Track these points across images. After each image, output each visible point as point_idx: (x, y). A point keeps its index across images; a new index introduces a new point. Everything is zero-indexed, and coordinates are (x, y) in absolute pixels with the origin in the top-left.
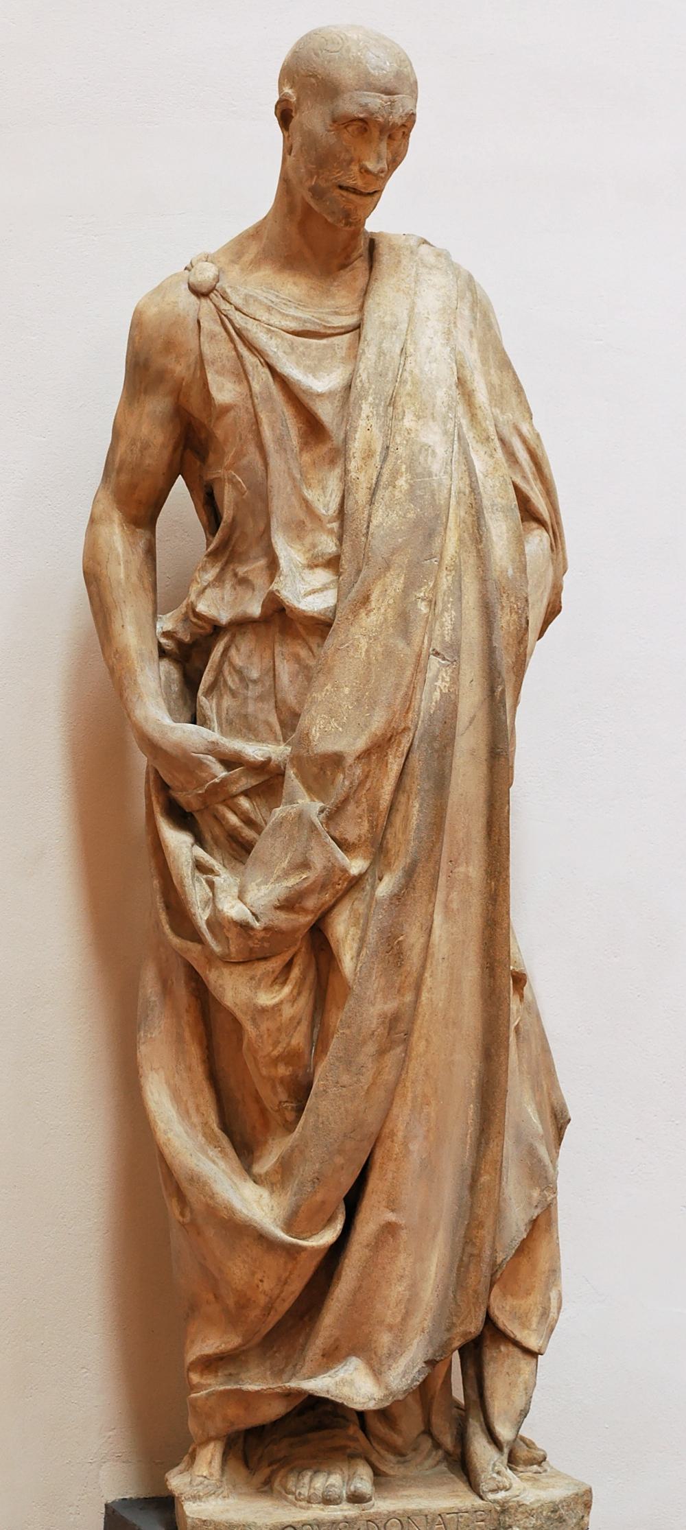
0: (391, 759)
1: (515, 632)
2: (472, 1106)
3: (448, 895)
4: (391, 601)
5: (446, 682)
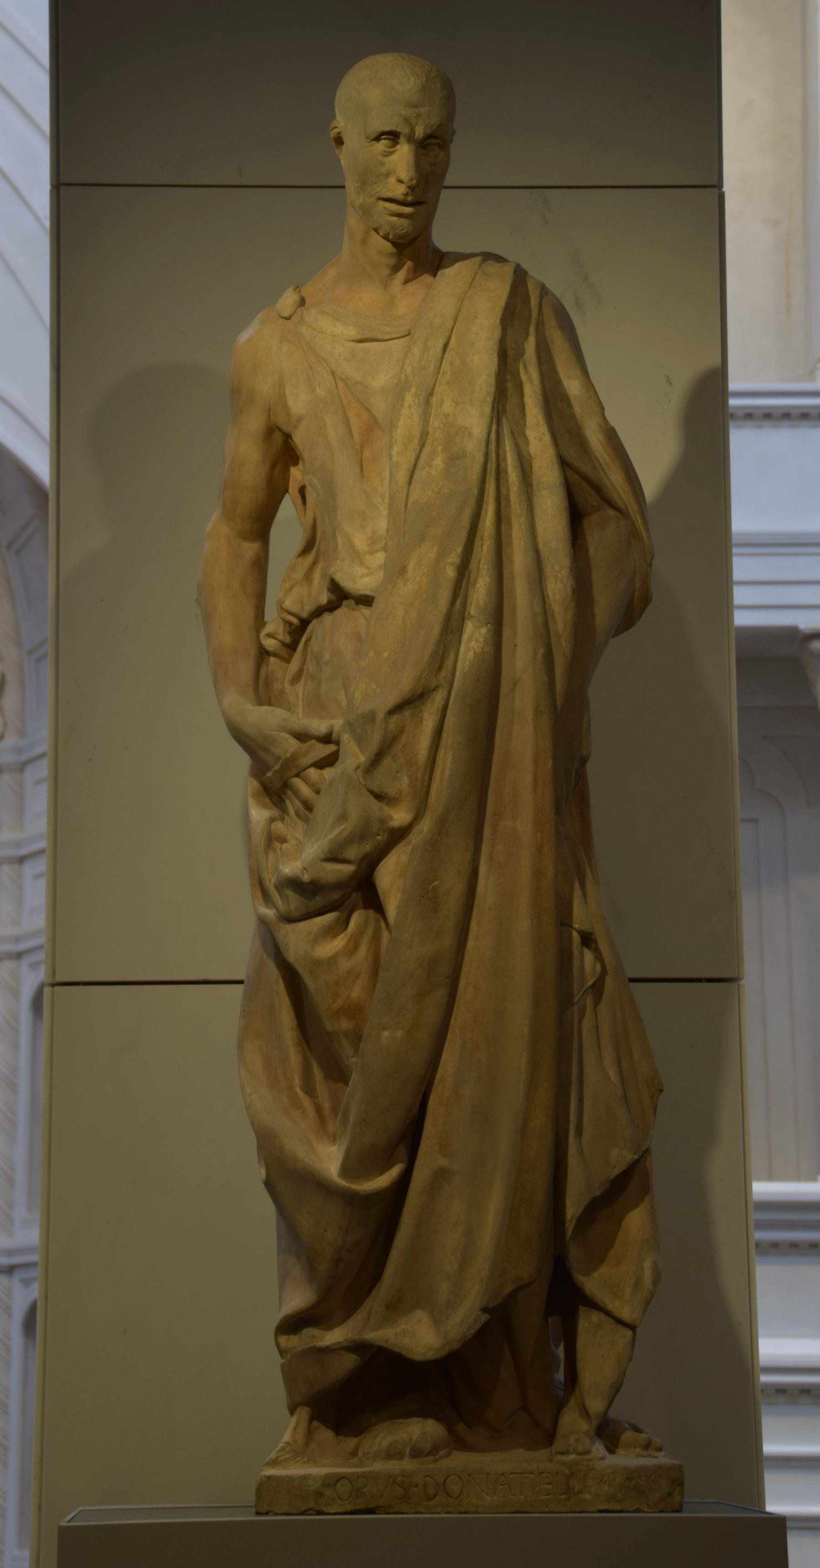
0: (426, 716)
2: (524, 1053)
4: (426, 570)
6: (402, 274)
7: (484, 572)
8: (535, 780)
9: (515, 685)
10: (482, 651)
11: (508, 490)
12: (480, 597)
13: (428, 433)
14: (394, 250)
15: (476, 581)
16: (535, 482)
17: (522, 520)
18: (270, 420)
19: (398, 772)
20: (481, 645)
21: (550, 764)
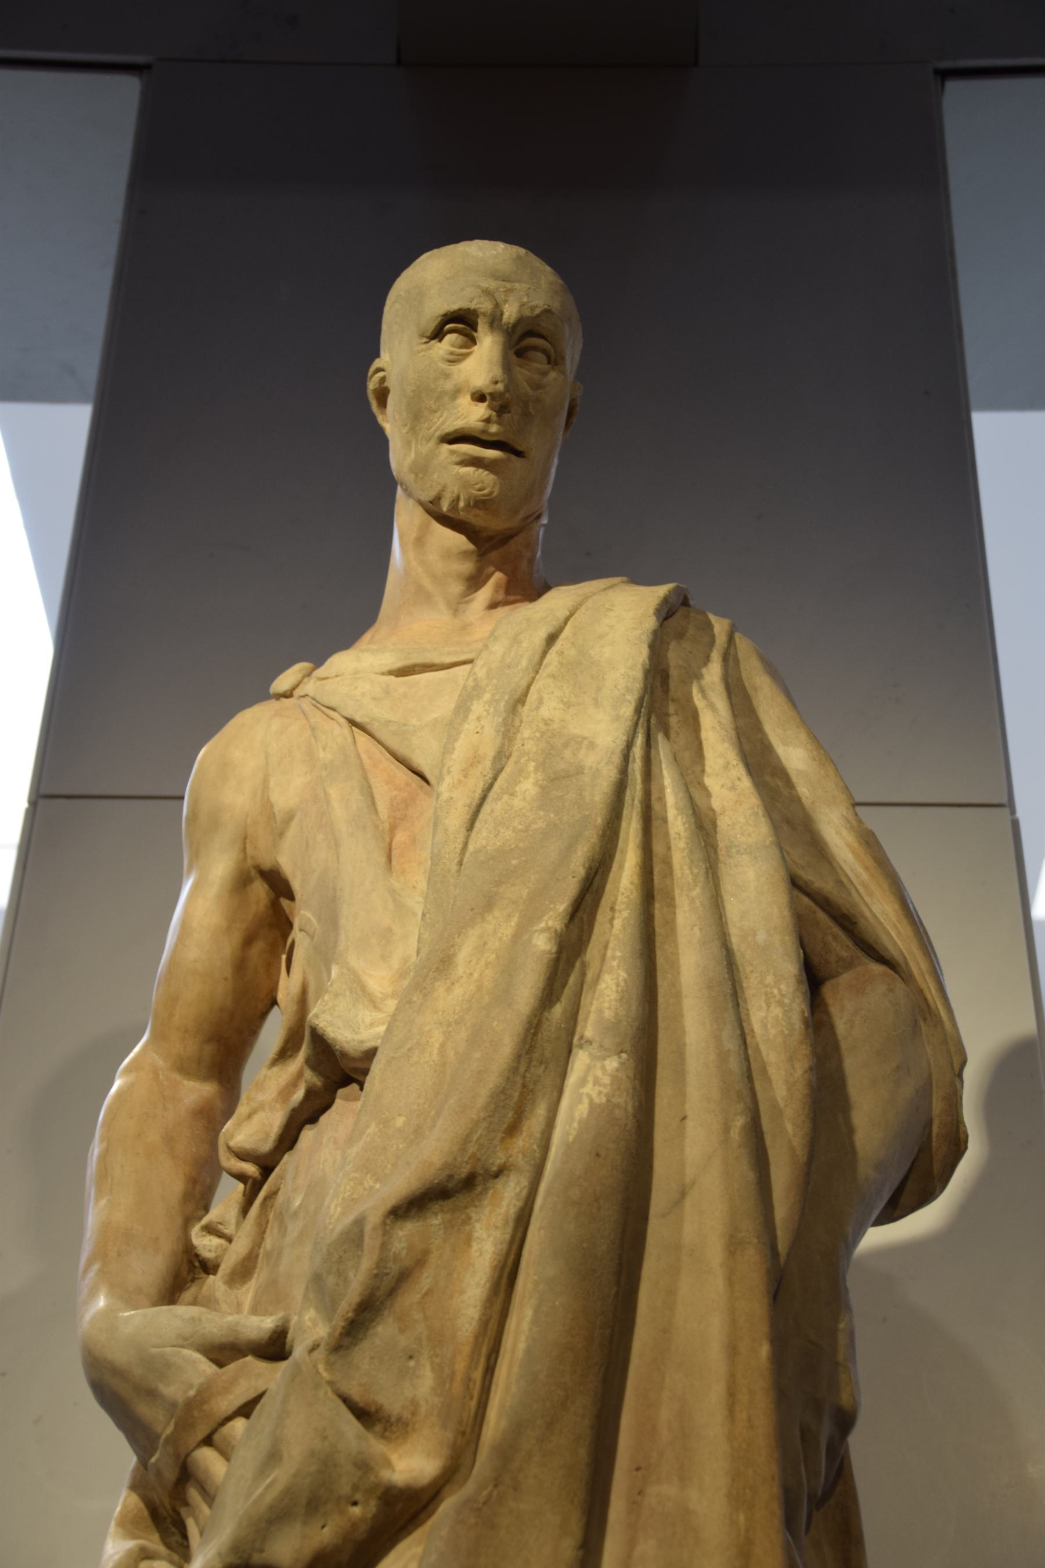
0: (479, 1230)
1: (780, 1039)
3: (631, 1543)
5: (605, 1086)
6: (485, 594)
7: (615, 963)
8: (731, 1393)
9: (683, 1194)
10: (608, 1101)
11: (669, 848)
12: (607, 1005)
13: (510, 755)
14: (470, 546)
15: (597, 979)
16: (721, 845)
17: (697, 892)
18: (245, 858)
19: (411, 1357)
20: (605, 1091)
21: (765, 1350)
